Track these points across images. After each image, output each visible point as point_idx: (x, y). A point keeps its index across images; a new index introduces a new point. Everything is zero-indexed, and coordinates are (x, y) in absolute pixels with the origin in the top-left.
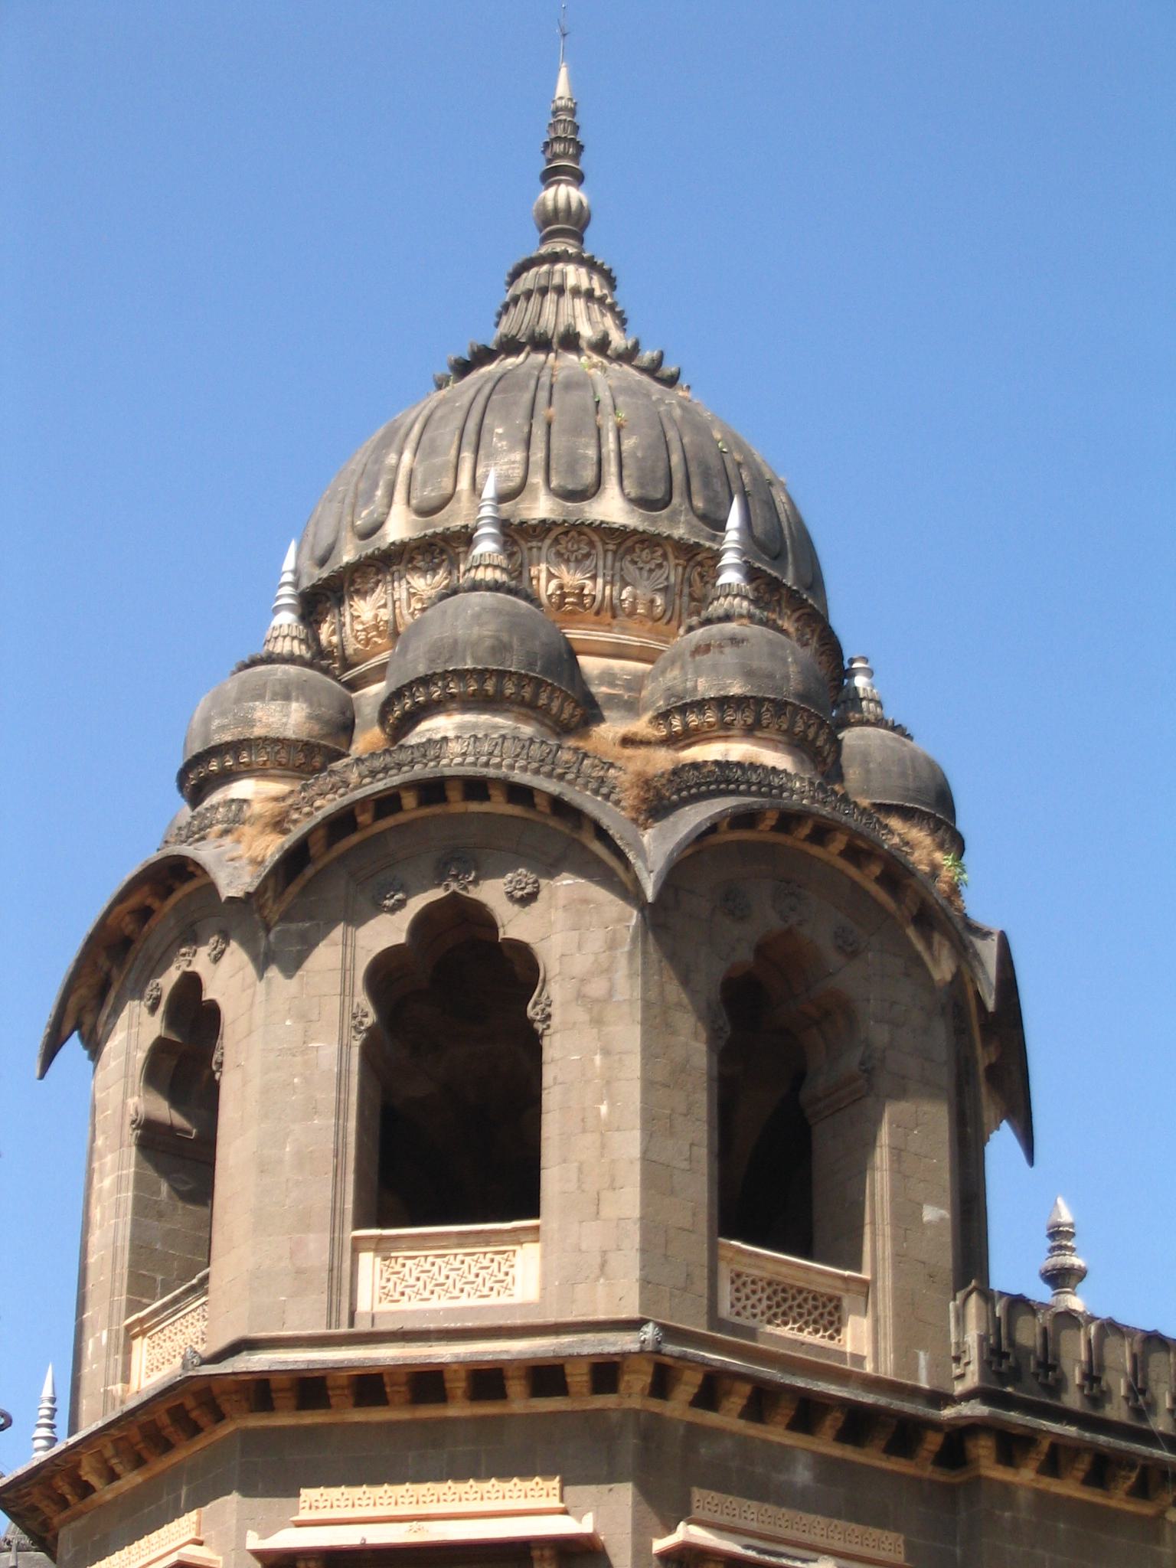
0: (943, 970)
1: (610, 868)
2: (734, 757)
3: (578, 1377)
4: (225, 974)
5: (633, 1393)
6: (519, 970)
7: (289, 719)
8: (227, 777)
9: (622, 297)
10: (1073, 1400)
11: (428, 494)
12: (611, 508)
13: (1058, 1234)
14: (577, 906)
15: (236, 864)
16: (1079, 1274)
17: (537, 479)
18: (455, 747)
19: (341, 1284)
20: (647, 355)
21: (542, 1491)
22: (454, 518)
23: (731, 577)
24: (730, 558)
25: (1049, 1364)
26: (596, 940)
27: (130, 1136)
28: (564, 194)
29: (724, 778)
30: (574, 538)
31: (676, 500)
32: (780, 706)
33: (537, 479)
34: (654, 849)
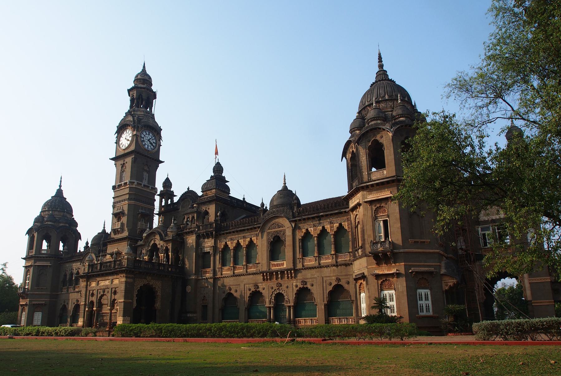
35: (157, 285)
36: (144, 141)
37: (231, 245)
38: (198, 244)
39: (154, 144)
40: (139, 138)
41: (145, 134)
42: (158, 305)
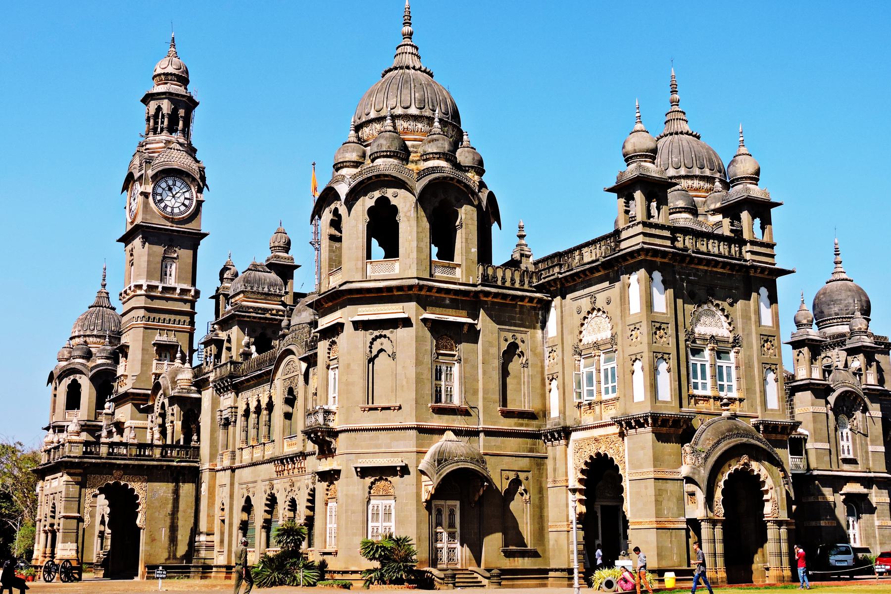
0: (476, 203)
1: (411, 191)
2: (436, 165)
4: (343, 210)
6: (394, 210)
7: (354, 156)
8: (342, 168)
9: (420, 53)
10: (499, 283)
11: (378, 108)
12: (413, 111)
13: (521, 228)
14: (405, 198)
15: (343, 190)
16: (525, 236)
17: (399, 104)
18: (382, 167)
20: (423, 69)
22: (382, 114)
23: (436, 120)
24: (436, 120)
25: (495, 277)
26: (408, 205)
27: (328, 237)
28: (407, 29)
29: (433, 170)
30: (407, 117)
31: (426, 106)
32: (444, 154)
33: (399, 104)
34: (419, 187)
36: (161, 201)
37: (253, 406)
38: (215, 404)
39: (187, 202)
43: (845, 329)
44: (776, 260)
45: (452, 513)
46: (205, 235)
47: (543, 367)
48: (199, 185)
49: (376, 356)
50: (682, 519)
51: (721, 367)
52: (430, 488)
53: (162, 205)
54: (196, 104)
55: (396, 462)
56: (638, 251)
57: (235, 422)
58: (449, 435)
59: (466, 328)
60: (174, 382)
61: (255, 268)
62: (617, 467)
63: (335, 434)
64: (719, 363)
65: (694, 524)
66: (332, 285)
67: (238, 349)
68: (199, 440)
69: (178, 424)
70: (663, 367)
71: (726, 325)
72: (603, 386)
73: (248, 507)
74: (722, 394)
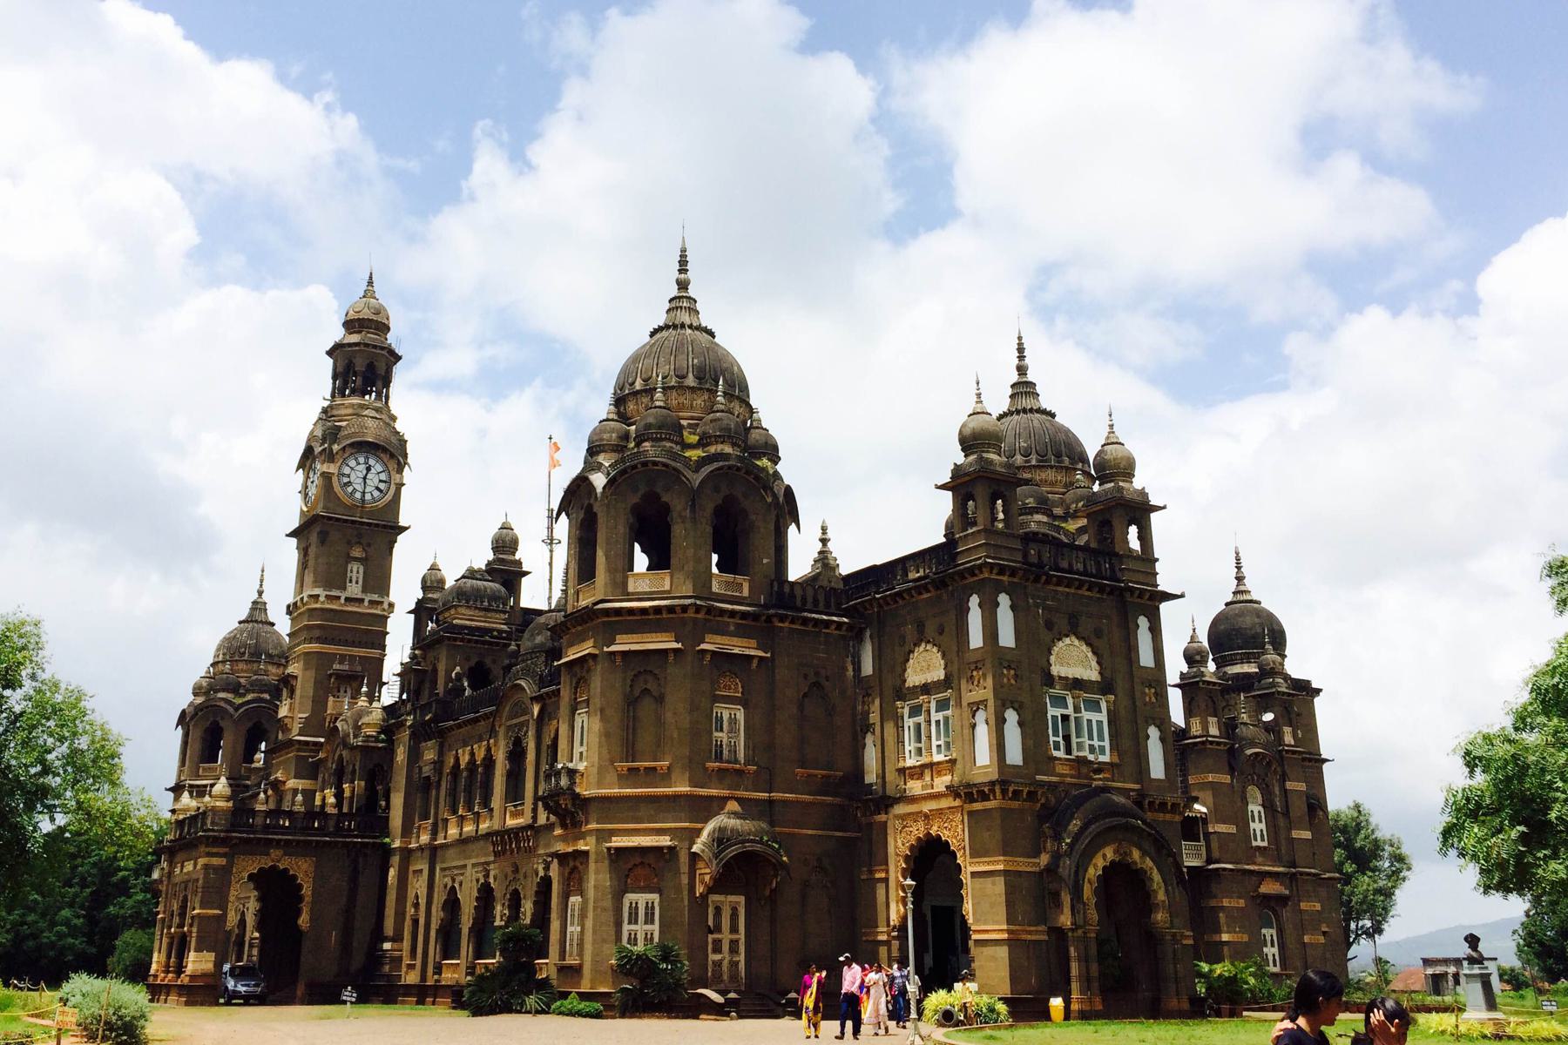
3: (678, 610)
5: (691, 614)
6: (666, 509)
10: (799, 603)
19: (625, 584)
21: (671, 636)
25: (792, 596)
35: (302, 869)
37: (464, 760)
38: (414, 755)
39: (382, 486)
40: (335, 479)
41: (352, 463)
42: (304, 920)
43: (1251, 668)
44: (1159, 579)
45: (734, 911)
46: (405, 529)
47: (854, 715)
48: (399, 463)
49: (636, 700)
50: (1042, 928)
51: (1089, 721)
52: (707, 878)
53: (350, 489)
54: (399, 358)
55: (665, 841)
56: (980, 567)
57: (439, 782)
58: (733, 806)
59: (755, 663)
60: (357, 728)
61: (471, 574)
62: (954, 855)
63: (584, 803)
64: (1086, 715)
65: (1058, 933)
66: (583, 603)
67: (446, 684)
68: (388, 806)
69: (360, 784)
70: (1011, 716)
71: (1094, 664)
72: (935, 743)
73: (452, 904)
74: (1091, 757)
